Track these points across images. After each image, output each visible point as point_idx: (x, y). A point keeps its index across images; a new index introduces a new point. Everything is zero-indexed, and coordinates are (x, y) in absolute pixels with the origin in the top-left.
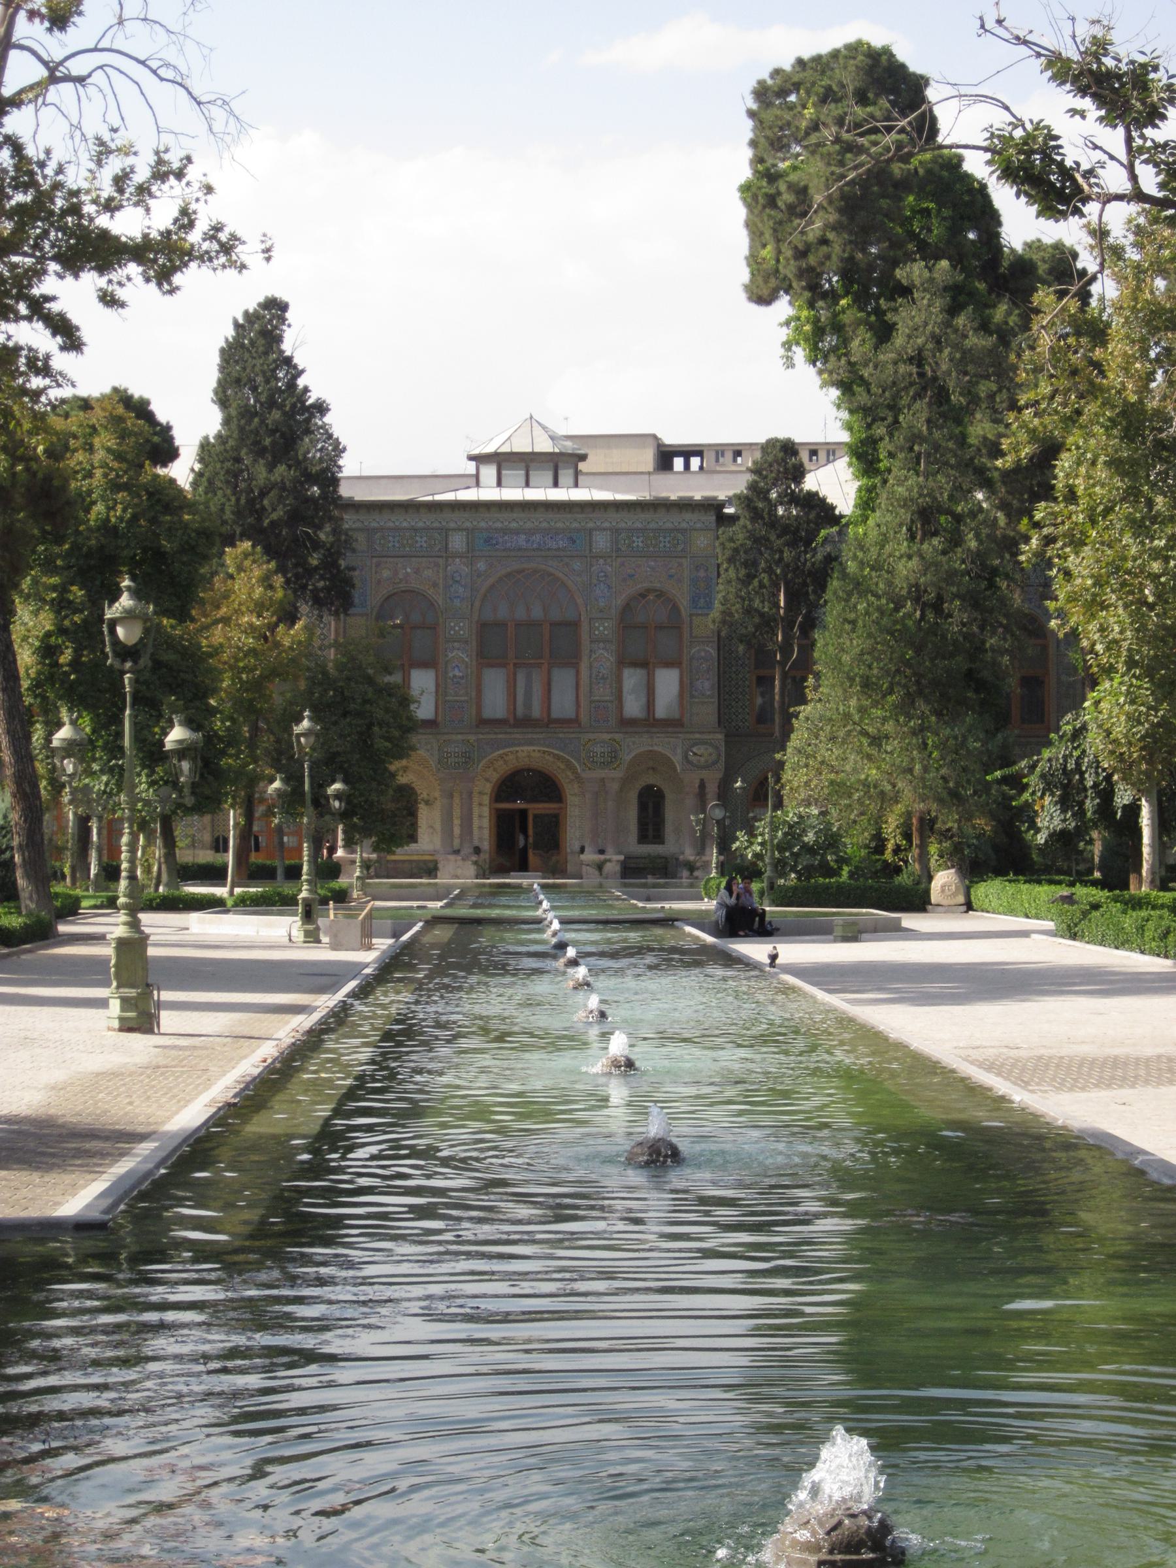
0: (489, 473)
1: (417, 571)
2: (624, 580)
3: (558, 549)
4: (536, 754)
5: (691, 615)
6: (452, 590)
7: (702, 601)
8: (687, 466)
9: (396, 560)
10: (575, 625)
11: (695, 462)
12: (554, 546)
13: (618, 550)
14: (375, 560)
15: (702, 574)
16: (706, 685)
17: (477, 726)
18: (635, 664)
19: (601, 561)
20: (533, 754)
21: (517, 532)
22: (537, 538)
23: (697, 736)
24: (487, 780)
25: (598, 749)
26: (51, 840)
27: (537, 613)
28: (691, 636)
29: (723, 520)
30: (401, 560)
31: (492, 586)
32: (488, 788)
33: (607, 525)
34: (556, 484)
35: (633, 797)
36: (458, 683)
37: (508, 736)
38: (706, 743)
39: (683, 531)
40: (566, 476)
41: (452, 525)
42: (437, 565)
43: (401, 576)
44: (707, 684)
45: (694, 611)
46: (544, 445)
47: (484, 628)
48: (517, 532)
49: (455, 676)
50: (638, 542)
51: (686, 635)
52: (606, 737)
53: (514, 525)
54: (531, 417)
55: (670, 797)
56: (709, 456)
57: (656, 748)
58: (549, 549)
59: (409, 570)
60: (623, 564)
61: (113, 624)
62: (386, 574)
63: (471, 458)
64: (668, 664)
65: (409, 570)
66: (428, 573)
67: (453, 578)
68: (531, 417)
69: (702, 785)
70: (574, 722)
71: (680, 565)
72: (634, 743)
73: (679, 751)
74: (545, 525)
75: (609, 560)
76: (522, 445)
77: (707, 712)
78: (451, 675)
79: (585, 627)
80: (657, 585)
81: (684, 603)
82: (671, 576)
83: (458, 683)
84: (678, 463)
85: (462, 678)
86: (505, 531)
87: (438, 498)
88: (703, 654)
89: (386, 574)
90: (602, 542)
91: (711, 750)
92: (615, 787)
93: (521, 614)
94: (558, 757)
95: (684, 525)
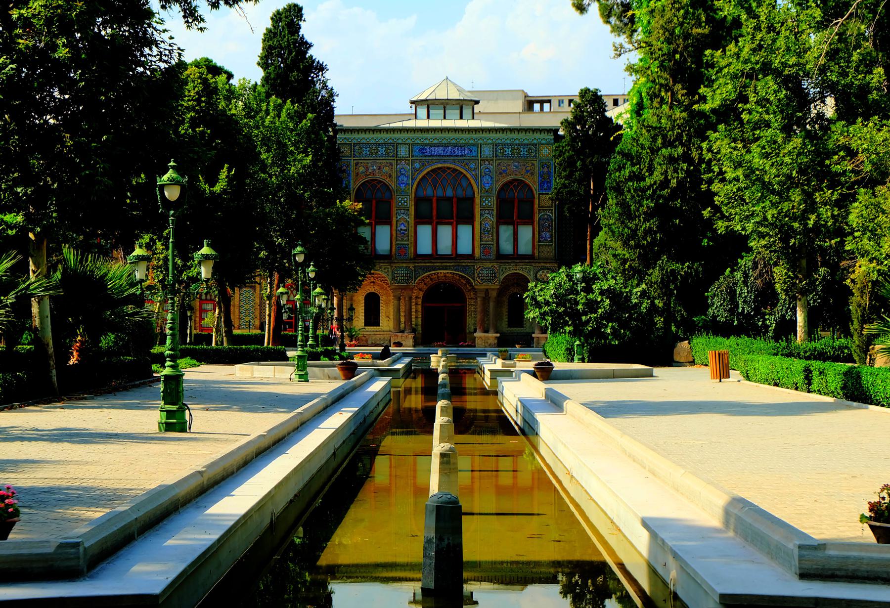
0: (422, 111)
1: (380, 168)
2: (500, 173)
3: (462, 156)
4: (450, 275)
5: (539, 194)
6: (400, 179)
7: (546, 185)
8: (542, 108)
9: (367, 161)
10: (472, 199)
11: (546, 106)
12: (460, 154)
13: (496, 156)
15: (546, 170)
17: (414, 259)
20: (447, 275)
21: (438, 146)
22: (449, 149)
23: (542, 264)
24: (420, 290)
25: (485, 272)
27: (449, 193)
28: (539, 207)
29: (558, 138)
30: (371, 161)
31: (424, 177)
32: (421, 294)
33: (490, 141)
34: (461, 118)
36: (403, 233)
37: (432, 265)
38: (548, 269)
39: (535, 145)
40: (467, 112)
41: (400, 141)
42: (391, 164)
43: (370, 171)
44: (548, 234)
45: (541, 192)
46: (454, 95)
47: (418, 201)
48: (438, 146)
49: (401, 229)
50: (508, 151)
51: (536, 206)
52: (490, 265)
53: (436, 142)
54: (447, 78)
56: (555, 103)
57: (518, 271)
58: (456, 156)
59: (375, 168)
60: (499, 164)
61: (162, 187)
62: (361, 169)
65: (375, 168)
66: (386, 169)
67: (400, 171)
68: (447, 78)
70: (471, 257)
71: (533, 164)
72: (506, 269)
73: (532, 273)
74: (453, 141)
75: (491, 162)
76: (441, 95)
77: (549, 251)
78: (399, 228)
79: (477, 201)
80: (519, 177)
81: (535, 187)
82: (528, 171)
83: (403, 233)
84: (537, 107)
85: (406, 230)
86: (431, 145)
87: (392, 125)
88: (546, 216)
89: (361, 169)
90: (487, 151)
92: (494, 294)
93: (440, 193)
94: (462, 277)
95: (535, 142)
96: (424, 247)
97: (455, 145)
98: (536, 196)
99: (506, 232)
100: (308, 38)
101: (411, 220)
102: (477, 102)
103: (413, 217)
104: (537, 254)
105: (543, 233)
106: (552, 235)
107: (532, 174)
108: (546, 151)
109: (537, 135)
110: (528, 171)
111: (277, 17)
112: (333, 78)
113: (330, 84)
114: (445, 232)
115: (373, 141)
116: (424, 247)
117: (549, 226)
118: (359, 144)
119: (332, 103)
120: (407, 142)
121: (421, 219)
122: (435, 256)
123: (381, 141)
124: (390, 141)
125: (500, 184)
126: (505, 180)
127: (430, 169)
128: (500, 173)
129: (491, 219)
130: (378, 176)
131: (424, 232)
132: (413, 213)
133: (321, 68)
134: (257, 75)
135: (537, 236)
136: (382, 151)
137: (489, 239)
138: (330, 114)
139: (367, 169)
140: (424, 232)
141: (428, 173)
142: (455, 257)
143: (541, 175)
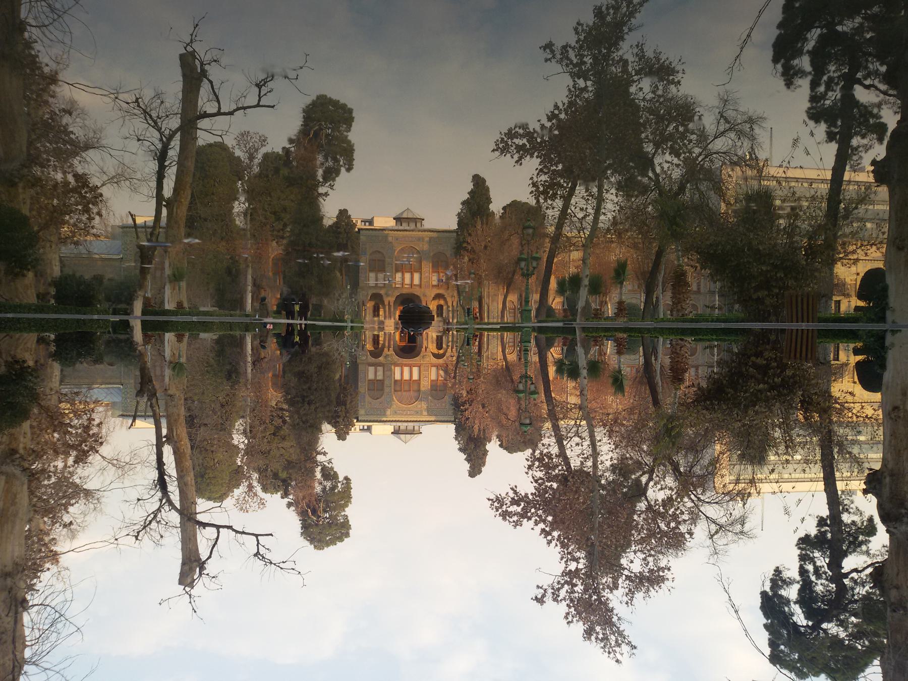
11: (361, 428)
16: (361, 376)
18: (380, 380)
26: (665, 466)
27: (404, 393)
40: (397, 428)
46: (402, 436)
77: (361, 367)
81: (367, 396)
97: (402, 414)
99: (380, 376)
101: (422, 382)
108: (362, 412)
109: (366, 419)
111: (480, 472)
112: (455, 445)
113: (457, 442)
114: (406, 376)
129: (387, 382)
130: (436, 401)
133: (460, 450)
134: (489, 446)
137: (388, 373)
138: (457, 430)
140: (415, 377)
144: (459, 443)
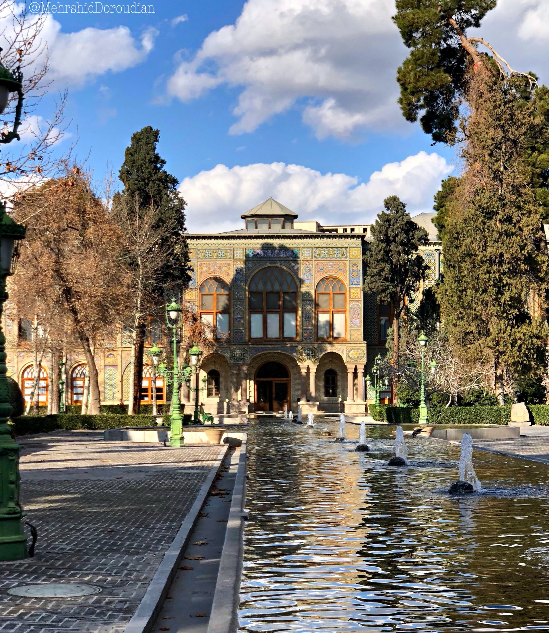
1: (219, 268)
2: (318, 271)
7: (355, 281)
14: (199, 263)
15: (355, 268)
19: (307, 263)
35: (322, 374)
38: (357, 349)
41: (236, 246)
42: (229, 265)
45: (352, 286)
49: (238, 318)
50: (324, 253)
55: (339, 375)
59: (215, 267)
60: (317, 264)
62: (205, 269)
63: (243, 218)
64: (339, 312)
65: (215, 267)
66: (224, 269)
69: (356, 369)
73: (345, 352)
75: (311, 262)
80: (334, 274)
81: (347, 283)
82: (341, 270)
91: (360, 352)
93: (269, 288)
95: (346, 245)
96: (257, 332)
98: (348, 289)
100: (162, 157)
102: (295, 217)
103: (247, 307)
104: (348, 337)
105: (354, 320)
106: (360, 322)
107: (344, 272)
110: (341, 270)
114: (273, 319)
115: (214, 246)
116: (257, 332)
117: (359, 314)
118: (203, 248)
119: (182, 211)
120: (242, 246)
121: (253, 309)
122: (265, 339)
123: (221, 246)
124: (228, 246)
125: (319, 280)
126: (322, 277)
127: (261, 268)
128: (318, 271)
131: (256, 319)
132: (247, 304)
135: (348, 322)
136: (221, 253)
139: (209, 268)
141: (259, 271)
142: (282, 340)
143: (352, 272)
144: (176, 194)
